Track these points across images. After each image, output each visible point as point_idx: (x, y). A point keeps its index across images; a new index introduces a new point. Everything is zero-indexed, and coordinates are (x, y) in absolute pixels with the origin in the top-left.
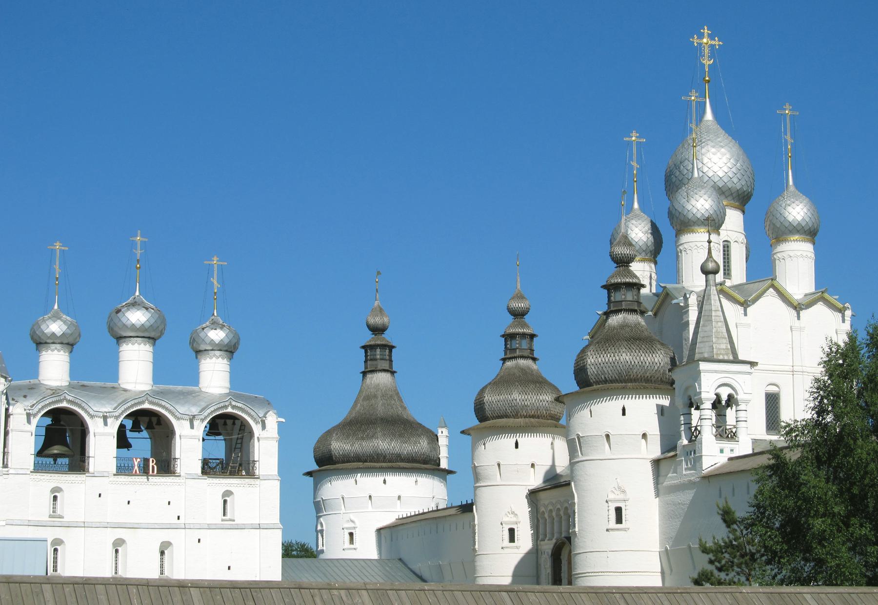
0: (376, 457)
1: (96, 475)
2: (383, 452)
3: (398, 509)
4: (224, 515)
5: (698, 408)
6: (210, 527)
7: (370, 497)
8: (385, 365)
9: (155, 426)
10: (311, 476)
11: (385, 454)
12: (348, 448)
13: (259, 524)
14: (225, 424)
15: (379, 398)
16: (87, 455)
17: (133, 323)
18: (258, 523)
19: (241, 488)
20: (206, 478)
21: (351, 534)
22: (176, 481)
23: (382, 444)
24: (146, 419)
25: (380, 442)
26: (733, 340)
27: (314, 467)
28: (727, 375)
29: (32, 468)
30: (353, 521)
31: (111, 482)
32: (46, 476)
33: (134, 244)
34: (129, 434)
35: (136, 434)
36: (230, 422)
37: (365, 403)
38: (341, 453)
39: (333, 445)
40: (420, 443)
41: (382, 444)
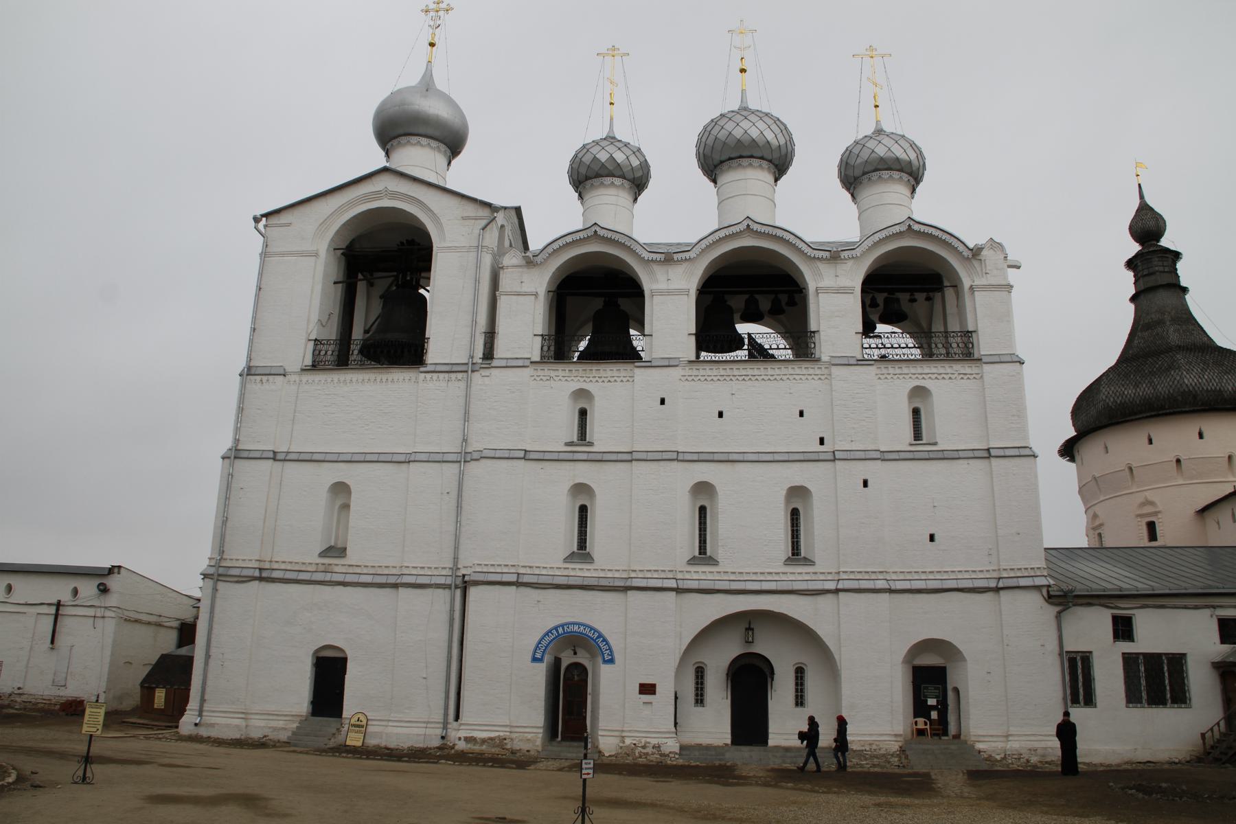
0: (1180, 398)
1: (653, 364)
2: (1191, 388)
4: (917, 435)
6: (885, 457)
7: (1178, 461)
9: (785, 308)
11: (1196, 392)
12: (1130, 392)
13: (988, 450)
15: (1168, 323)
17: (738, 137)
18: (986, 448)
22: (811, 371)
23: (1188, 376)
29: (537, 359)
30: (1152, 503)
31: (683, 379)
36: (921, 296)
38: (1119, 402)
39: (1104, 390)
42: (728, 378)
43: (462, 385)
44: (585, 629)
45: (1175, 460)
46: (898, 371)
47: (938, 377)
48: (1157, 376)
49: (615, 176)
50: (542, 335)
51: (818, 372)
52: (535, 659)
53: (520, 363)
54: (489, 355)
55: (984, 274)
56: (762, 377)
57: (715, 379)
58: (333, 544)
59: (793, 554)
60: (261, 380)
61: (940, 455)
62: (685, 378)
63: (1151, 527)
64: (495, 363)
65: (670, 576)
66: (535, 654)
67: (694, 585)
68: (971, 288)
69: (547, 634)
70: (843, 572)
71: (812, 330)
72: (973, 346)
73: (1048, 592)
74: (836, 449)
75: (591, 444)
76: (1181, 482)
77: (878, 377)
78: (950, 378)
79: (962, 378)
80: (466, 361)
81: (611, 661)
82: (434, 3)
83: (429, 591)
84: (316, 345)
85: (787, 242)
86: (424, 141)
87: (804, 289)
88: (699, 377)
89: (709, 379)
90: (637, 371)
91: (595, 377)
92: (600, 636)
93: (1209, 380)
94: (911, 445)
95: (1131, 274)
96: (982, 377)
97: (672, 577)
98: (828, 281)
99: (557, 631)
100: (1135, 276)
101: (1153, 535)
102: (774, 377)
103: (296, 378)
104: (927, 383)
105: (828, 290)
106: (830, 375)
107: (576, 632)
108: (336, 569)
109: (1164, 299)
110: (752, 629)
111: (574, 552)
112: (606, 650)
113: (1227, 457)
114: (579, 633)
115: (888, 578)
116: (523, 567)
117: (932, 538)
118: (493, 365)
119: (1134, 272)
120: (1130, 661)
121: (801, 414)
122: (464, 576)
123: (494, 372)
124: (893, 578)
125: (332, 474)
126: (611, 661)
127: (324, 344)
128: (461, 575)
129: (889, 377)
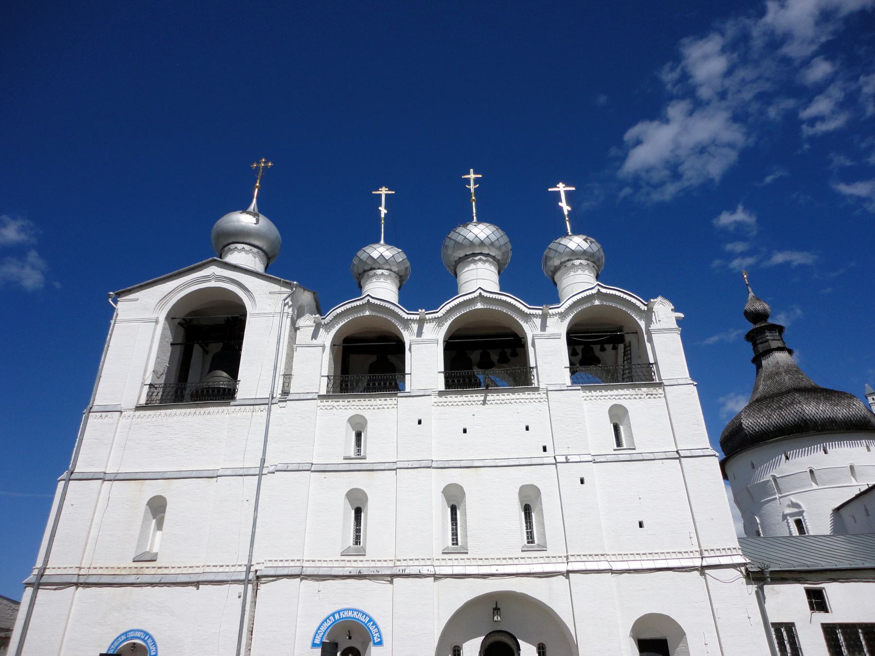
1: (412, 395)
2: (811, 417)
3: (854, 483)
4: (619, 443)
8: (779, 344)
9: (509, 357)
15: (783, 374)
18: (676, 450)
19: (638, 400)
20: (580, 388)
21: (799, 523)
22: (533, 396)
23: (807, 408)
25: (804, 406)
29: (323, 392)
32: (342, 403)
33: (468, 181)
37: (768, 383)
40: (854, 405)
41: (807, 408)
42: (469, 403)
43: (265, 413)
44: (358, 614)
45: (808, 470)
46: (600, 394)
47: (631, 397)
48: (783, 410)
49: (384, 269)
50: (328, 376)
51: (539, 396)
52: (314, 645)
53: (310, 396)
54: (285, 393)
55: (658, 322)
56: (495, 402)
57: (460, 404)
58: (148, 550)
59: (528, 543)
60: (101, 416)
62: (437, 404)
64: (289, 397)
65: (429, 563)
66: (314, 640)
67: (448, 571)
69: (325, 621)
70: (571, 556)
71: (531, 366)
72: (655, 375)
73: (746, 569)
74: (556, 454)
76: (817, 487)
77: (584, 399)
78: (640, 398)
79: (649, 398)
80: (268, 397)
81: (380, 643)
83: (226, 586)
84: (150, 388)
86: (247, 247)
87: (524, 338)
88: (448, 403)
89: (455, 404)
91: (368, 406)
92: (371, 620)
93: (823, 410)
94: (615, 450)
95: (750, 345)
96: (665, 396)
97: (430, 564)
99: (334, 618)
100: (753, 345)
102: (504, 402)
103: (131, 413)
106: (548, 398)
107: (350, 617)
108: (147, 571)
110: (499, 609)
111: (350, 547)
112: (376, 633)
113: (849, 466)
114: (353, 618)
115: (609, 560)
116: (307, 561)
117: (641, 525)
119: (752, 342)
120: (829, 630)
121: (527, 429)
122: (256, 571)
124: (613, 560)
125: (152, 489)
126: (380, 643)
127: (156, 388)
128: (254, 570)
129: (592, 398)
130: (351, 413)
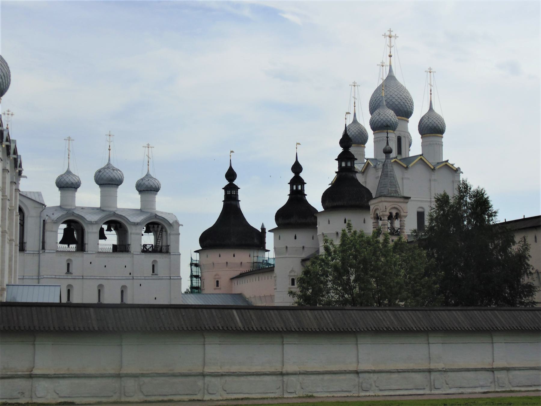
4: (153, 271)
5: (381, 220)
7: (227, 263)
10: (198, 253)
14: (154, 227)
16: (84, 243)
24: (114, 225)
26: (43, 232)
27: (200, 248)
28: (395, 203)
30: (218, 275)
34: (105, 232)
35: (109, 232)
36: (156, 226)
53: (53, 251)
61: (159, 278)
63: (218, 282)
68: (170, 234)
75: (71, 273)
82: (7, 111)
85: (124, 220)
90: (84, 254)
98: (134, 231)
101: (217, 285)
104: (157, 260)
105: (133, 234)
109: (233, 203)
118: (46, 251)
123: (46, 254)
130: (67, 258)
